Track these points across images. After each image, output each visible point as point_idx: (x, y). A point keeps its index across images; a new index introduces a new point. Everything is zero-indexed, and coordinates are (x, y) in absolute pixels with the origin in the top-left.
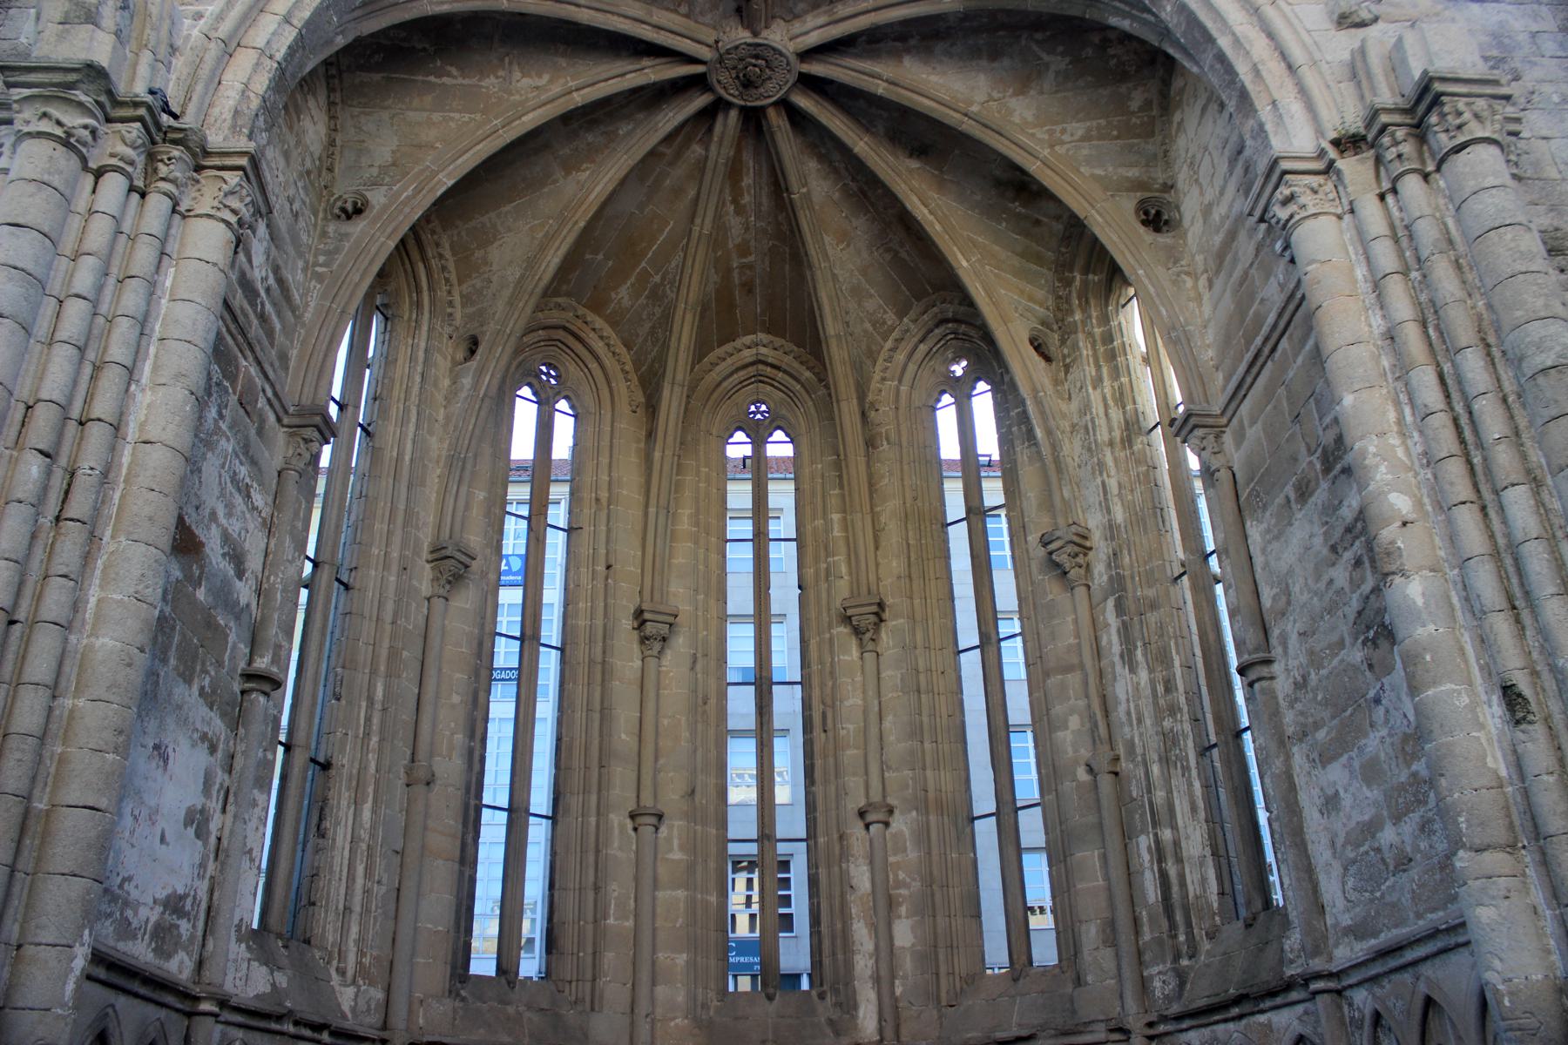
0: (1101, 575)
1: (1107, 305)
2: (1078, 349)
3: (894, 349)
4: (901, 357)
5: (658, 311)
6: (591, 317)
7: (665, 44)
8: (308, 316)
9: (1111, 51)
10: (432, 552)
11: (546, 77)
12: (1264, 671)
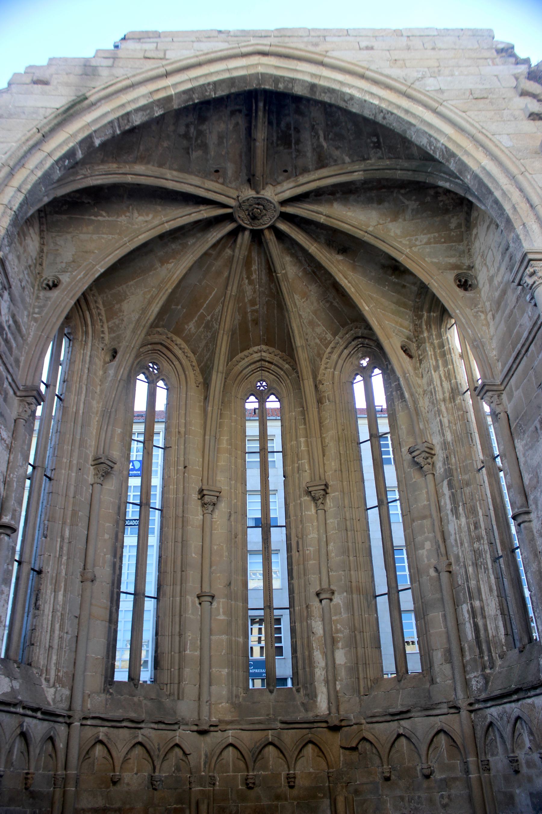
0: (440, 468)
1: (440, 329)
2: (426, 351)
3: (331, 353)
4: (335, 356)
5: (209, 334)
6: (175, 338)
7: (211, 198)
8: (30, 339)
9: (440, 199)
10: (94, 460)
11: (151, 216)
12: (526, 517)
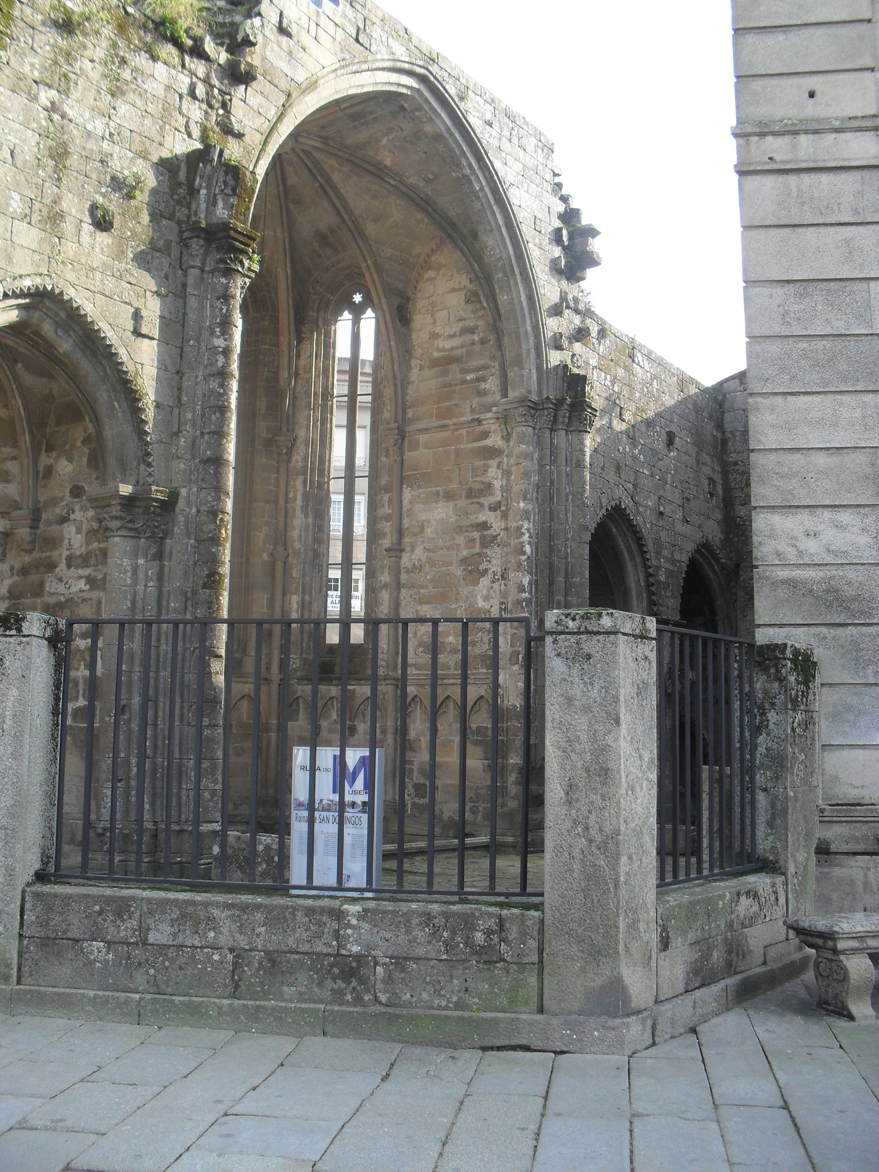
9: (421, 225)
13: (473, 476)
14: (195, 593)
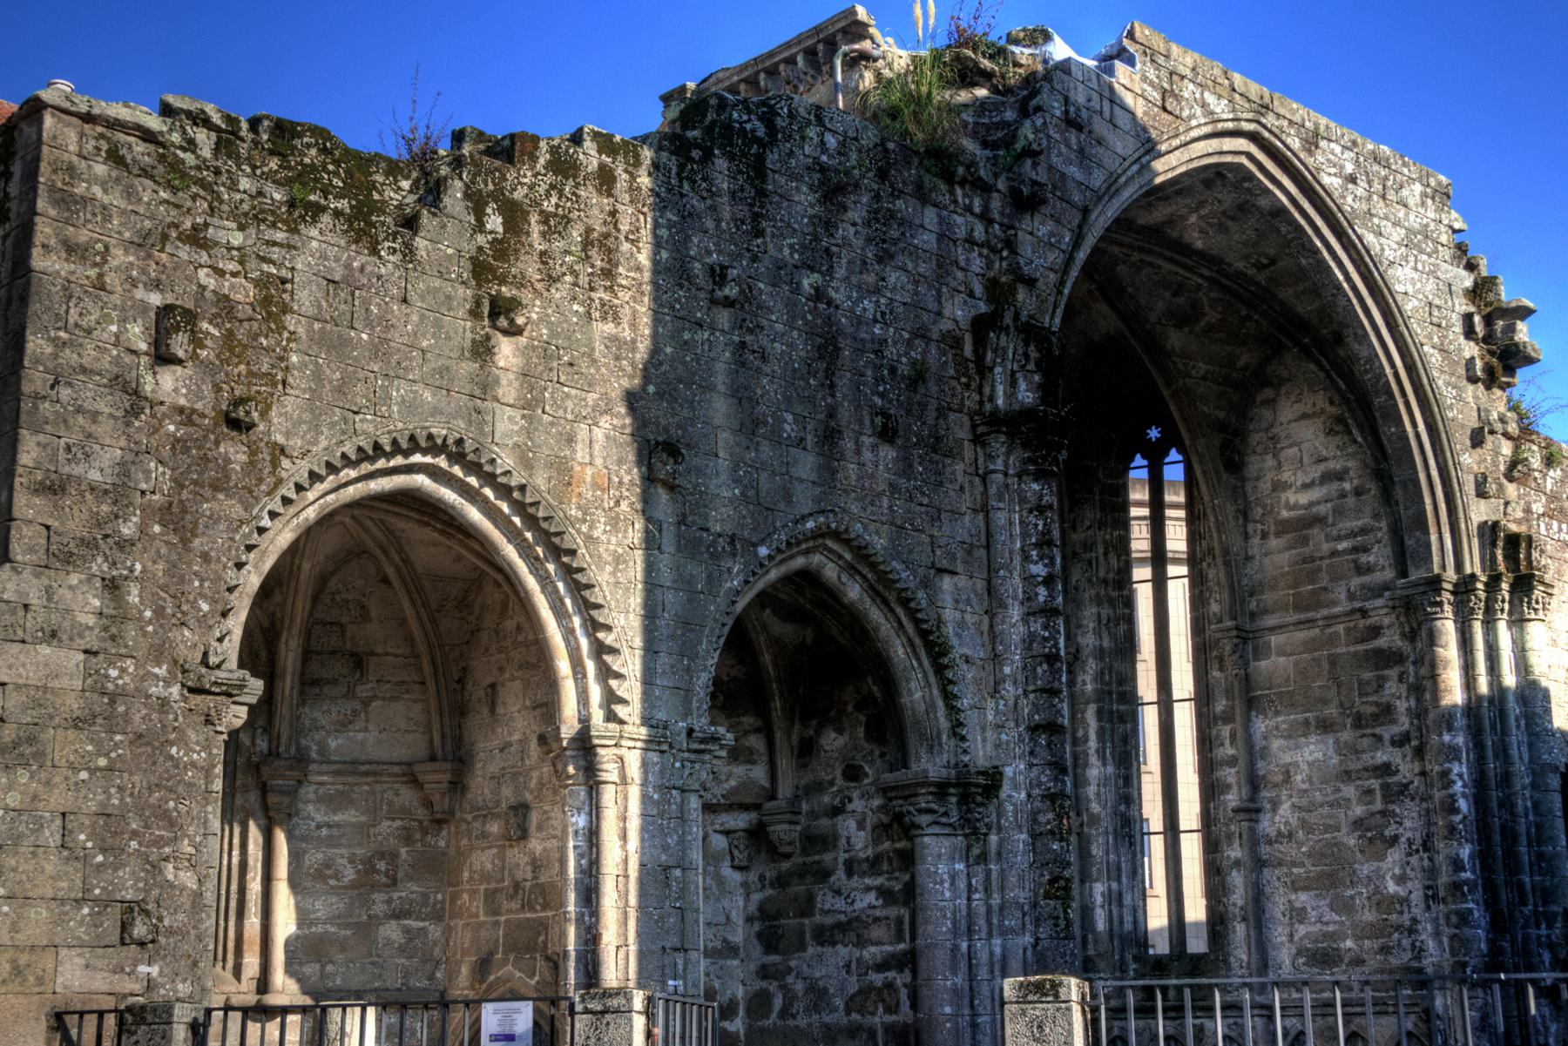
13: (1361, 695)
14: (1035, 905)
